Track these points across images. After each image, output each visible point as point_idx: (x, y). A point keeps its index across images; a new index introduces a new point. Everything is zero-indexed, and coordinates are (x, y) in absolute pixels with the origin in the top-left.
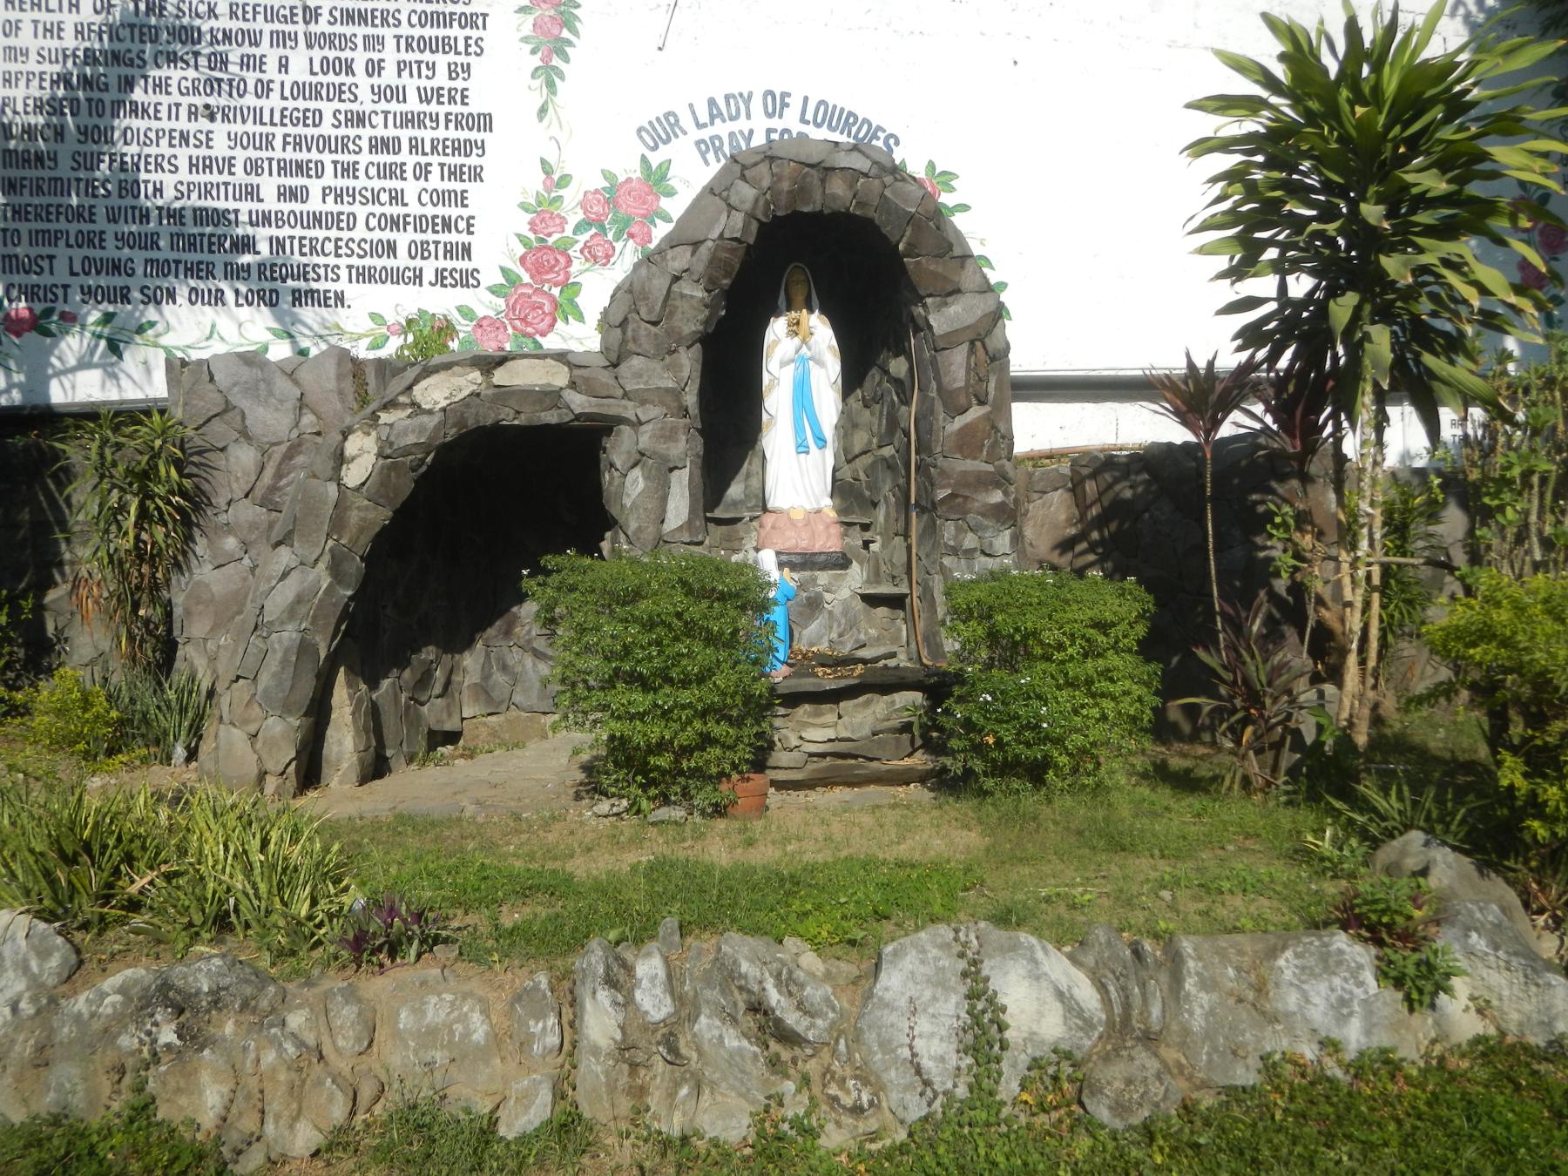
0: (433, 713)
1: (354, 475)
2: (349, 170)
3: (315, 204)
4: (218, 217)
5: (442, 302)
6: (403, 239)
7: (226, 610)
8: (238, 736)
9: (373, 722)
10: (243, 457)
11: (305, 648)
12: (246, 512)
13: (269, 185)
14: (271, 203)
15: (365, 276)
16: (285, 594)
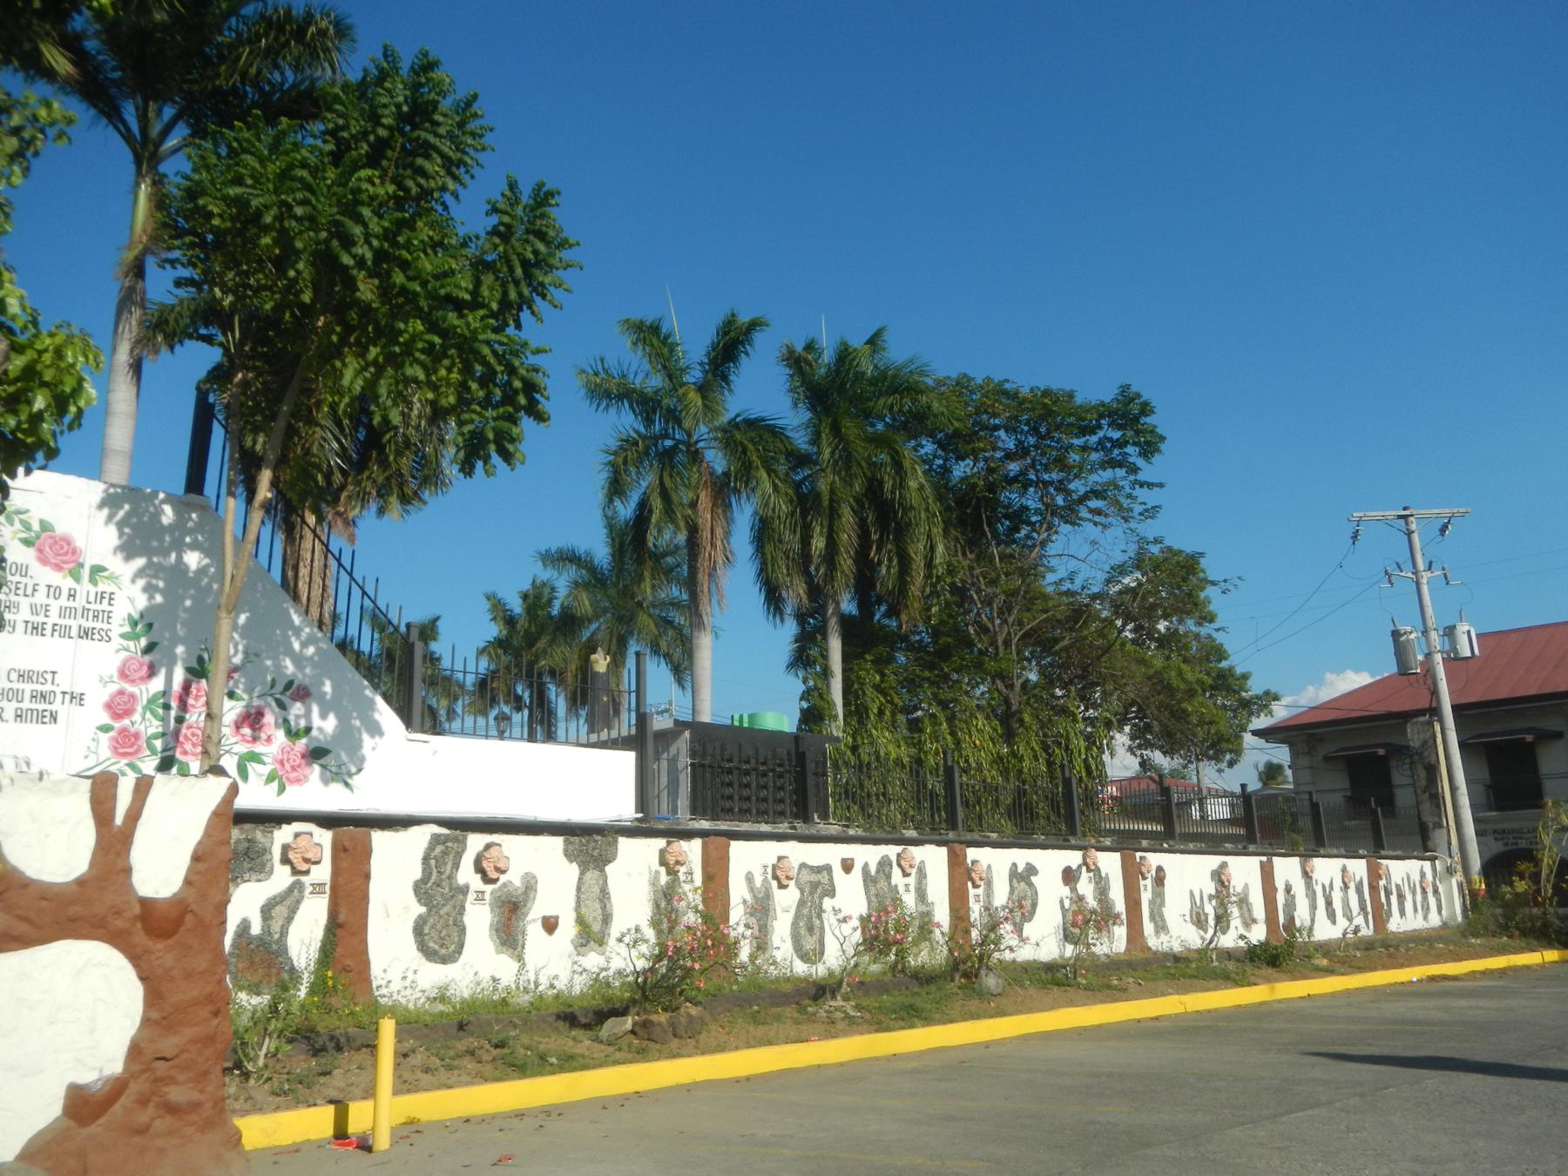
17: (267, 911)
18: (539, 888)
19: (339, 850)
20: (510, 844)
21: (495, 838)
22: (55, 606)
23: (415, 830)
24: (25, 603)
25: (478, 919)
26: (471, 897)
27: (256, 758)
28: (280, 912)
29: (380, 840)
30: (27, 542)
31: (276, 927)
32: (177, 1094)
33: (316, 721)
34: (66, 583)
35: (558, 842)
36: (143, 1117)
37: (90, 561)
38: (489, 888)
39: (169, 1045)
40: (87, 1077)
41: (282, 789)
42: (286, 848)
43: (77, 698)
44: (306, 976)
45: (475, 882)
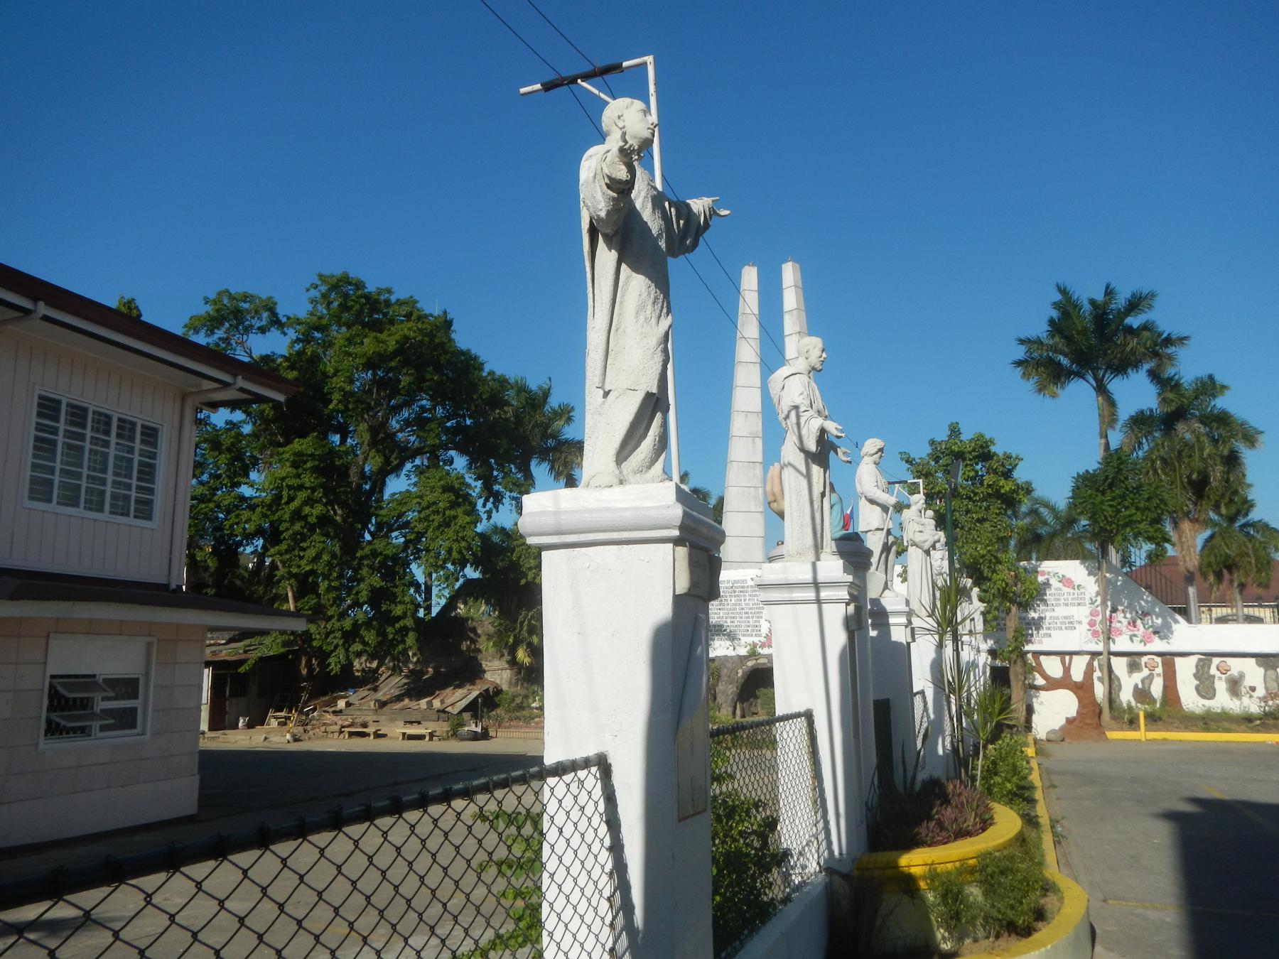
0: (753, 709)
1: (739, 675)
2: (741, 618)
3: (736, 624)
4: (721, 626)
5: (756, 640)
6: (750, 629)
7: (723, 692)
8: (725, 710)
9: (743, 710)
10: (725, 670)
11: (733, 698)
12: (726, 678)
13: (729, 620)
14: (729, 624)
15: (744, 635)
16: (730, 692)
17: (1143, 681)
18: (1246, 676)
19: (1164, 664)
20: (1230, 661)
21: (1224, 659)
22: (1070, 598)
23: (1191, 657)
24: (1062, 598)
25: (1221, 686)
26: (1216, 678)
27: (1135, 636)
28: (1147, 681)
29: (1178, 660)
30: (1060, 582)
31: (1146, 686)
32: (1088, 721)
33: (1155, 620)
34: (1072, 591)
35: (1253, 660)
36: (1080, 725)
37: (1076, 584)
38: (1224, 676)
39: (1085, 711)
40: (1069, 716)
41: (1145, 645)
42: (1146, 663)
43: (1080, 622)
44: (1158, 701)
45: (1218, 674)
